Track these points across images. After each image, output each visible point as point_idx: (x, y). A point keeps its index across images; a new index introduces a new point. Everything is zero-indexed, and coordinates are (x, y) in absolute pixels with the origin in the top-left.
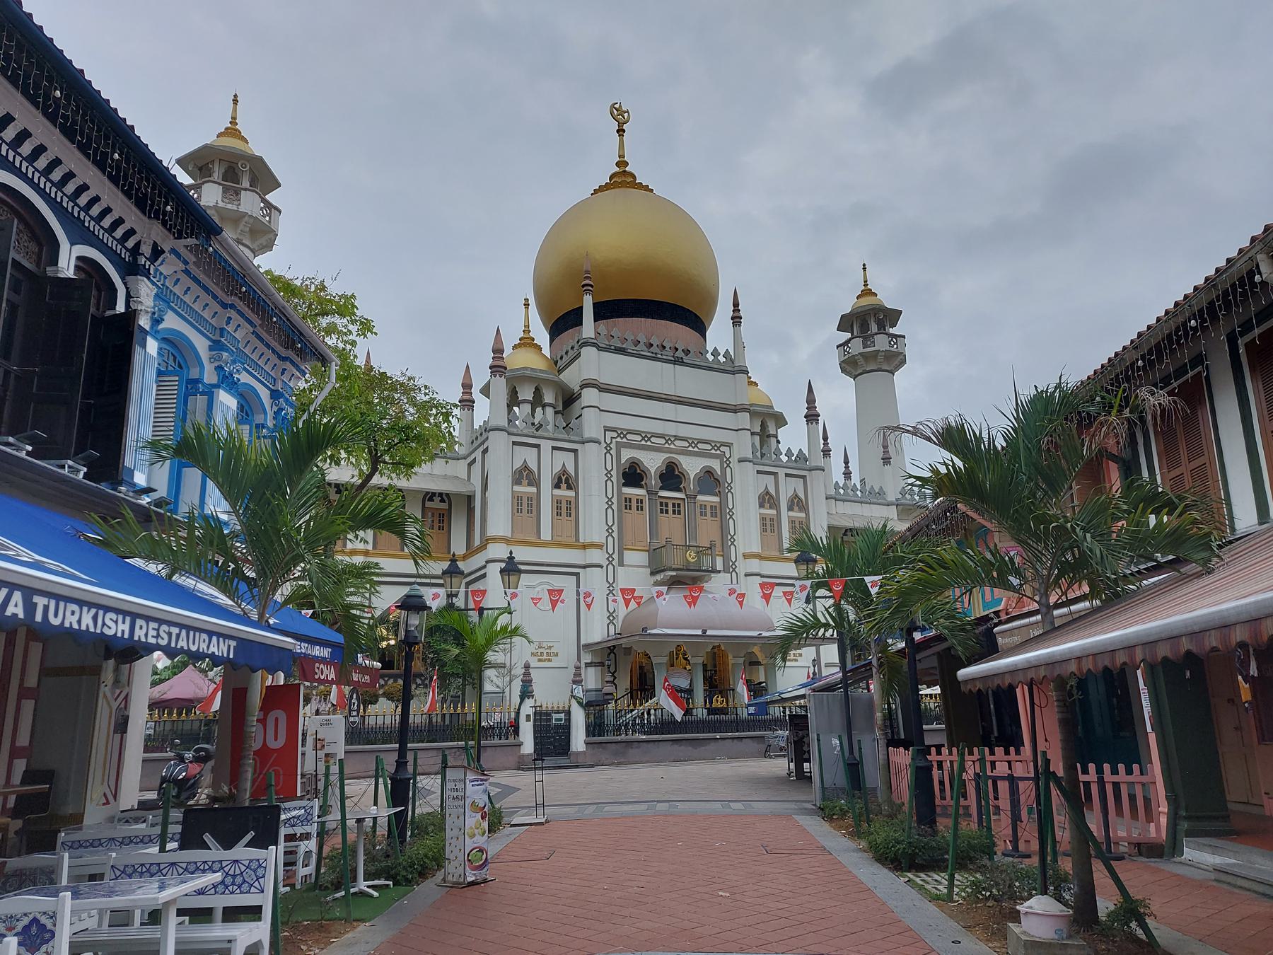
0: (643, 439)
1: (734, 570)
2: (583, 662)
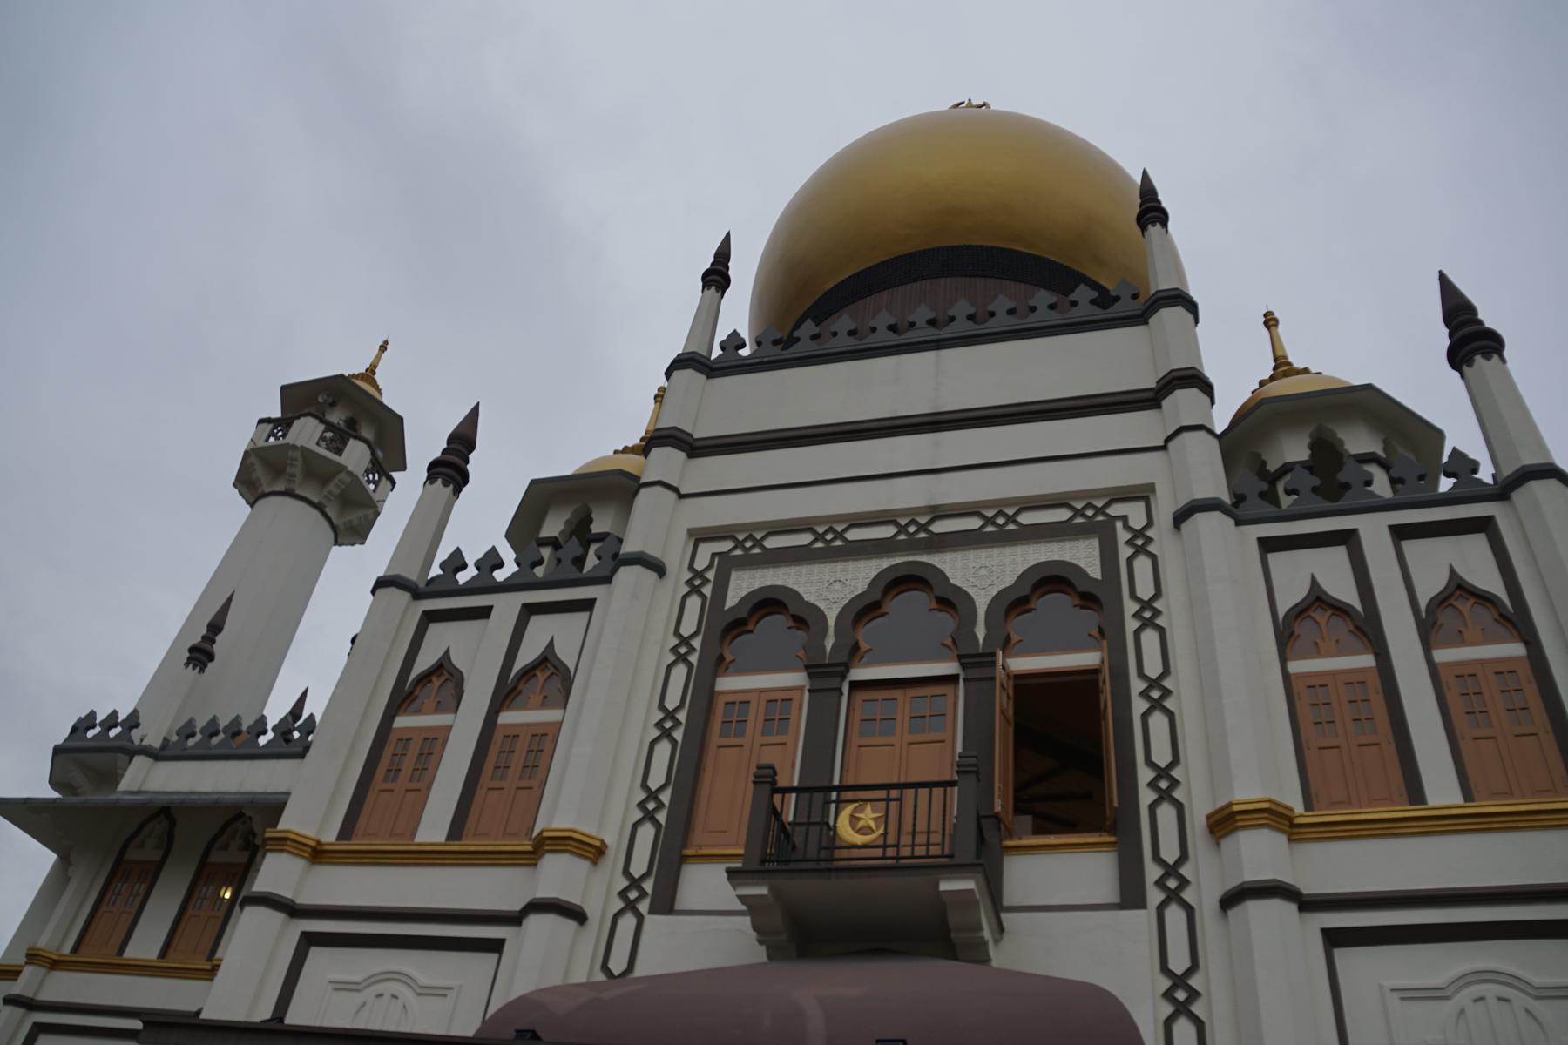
1: (1173, 896)
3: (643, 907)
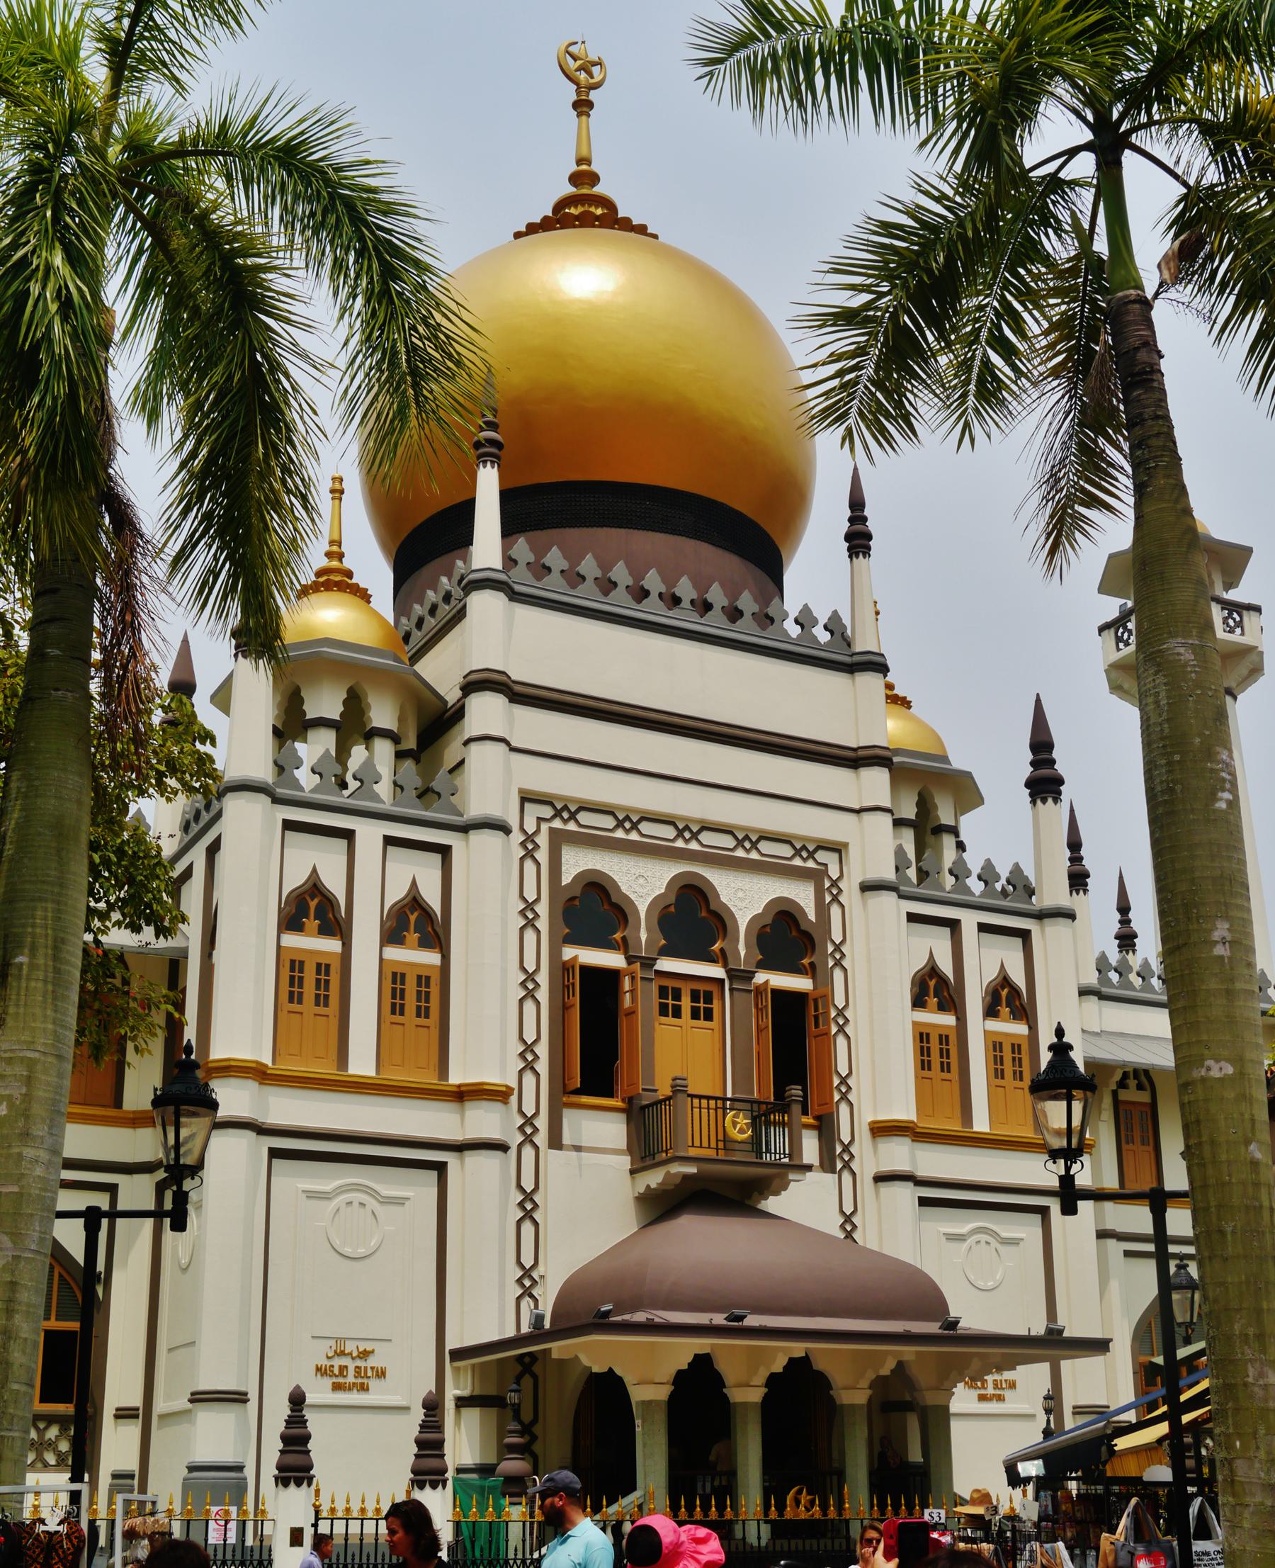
0: (620, 824)
1: (847, 1165)
2: (451, 1393)
3: (537, 1140)
